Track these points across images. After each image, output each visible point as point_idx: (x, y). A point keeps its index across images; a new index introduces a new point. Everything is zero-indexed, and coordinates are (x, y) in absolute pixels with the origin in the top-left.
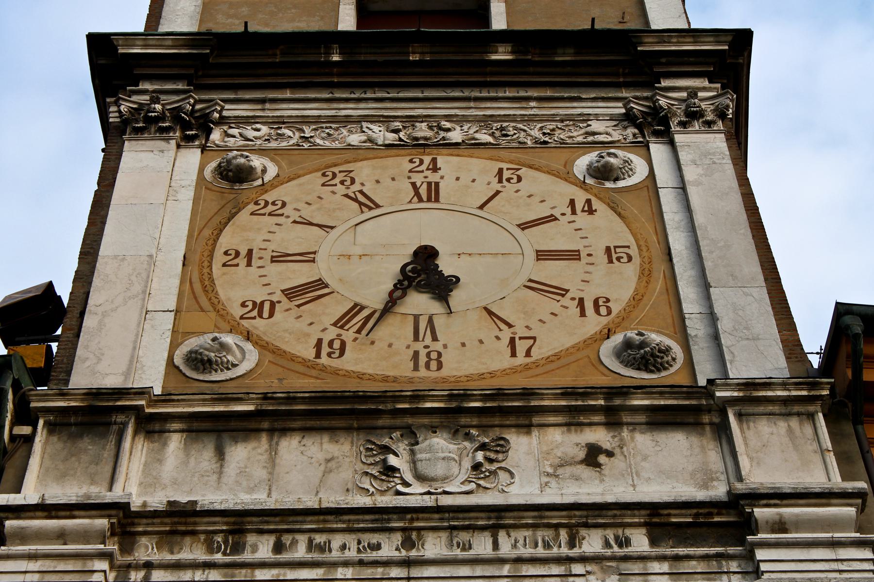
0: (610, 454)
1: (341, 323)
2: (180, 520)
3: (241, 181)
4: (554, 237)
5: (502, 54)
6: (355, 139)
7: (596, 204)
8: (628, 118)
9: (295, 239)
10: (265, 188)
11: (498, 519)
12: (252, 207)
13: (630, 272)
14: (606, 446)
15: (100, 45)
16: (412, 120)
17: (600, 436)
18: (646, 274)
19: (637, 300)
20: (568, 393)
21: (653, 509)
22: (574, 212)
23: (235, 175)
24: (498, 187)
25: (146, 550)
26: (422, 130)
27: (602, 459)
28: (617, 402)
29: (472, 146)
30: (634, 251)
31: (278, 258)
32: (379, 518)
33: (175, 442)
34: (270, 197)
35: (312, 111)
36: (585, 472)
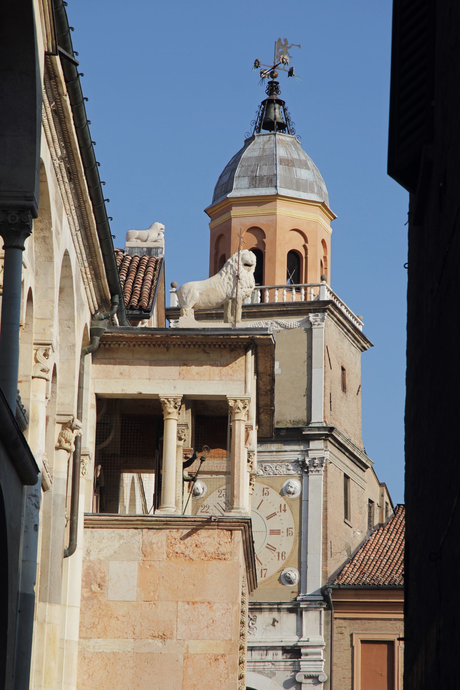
0: (277, 622)
3: (198, 495)
4: (274, 524)
7: (287, 508)
10: (204, 499)
12: (201, 508)
14: (277, 619)
17: (275, 615)
19: (292, 553)
20: (269, 604)
21: (283, 647)
22: (281, 512)
24: (262, 498)
27: (276, 623)
28: (280, 606)
30: (293, 530)
34: (205, 503)
36: (272, 627)
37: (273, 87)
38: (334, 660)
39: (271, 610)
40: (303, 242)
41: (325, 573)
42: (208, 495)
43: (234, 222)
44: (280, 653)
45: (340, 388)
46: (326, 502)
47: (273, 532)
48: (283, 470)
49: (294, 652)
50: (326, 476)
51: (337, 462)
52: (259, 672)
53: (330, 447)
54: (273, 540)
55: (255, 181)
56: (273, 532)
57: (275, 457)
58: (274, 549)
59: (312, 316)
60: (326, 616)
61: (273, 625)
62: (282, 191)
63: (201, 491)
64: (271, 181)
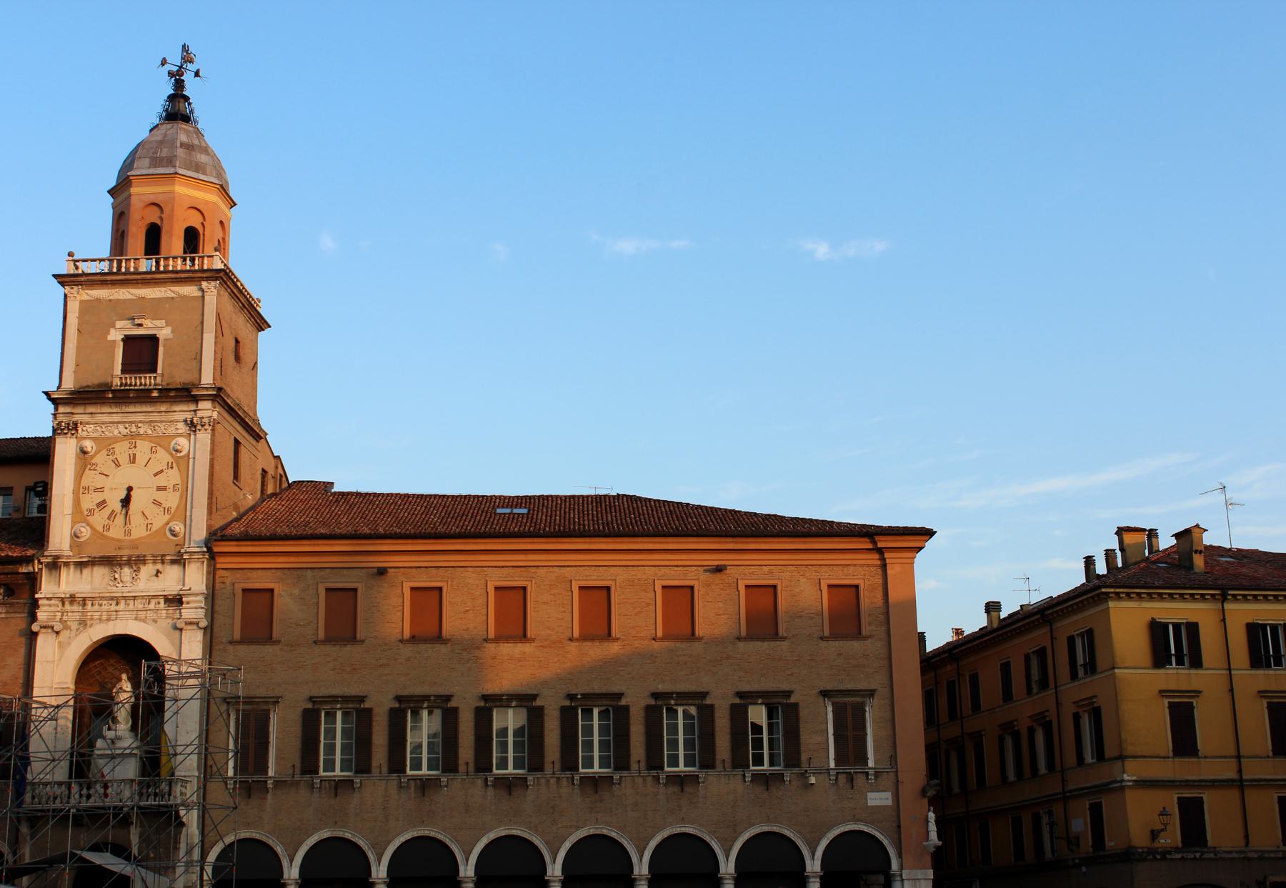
1: (109, 518)
2: (72, 598)
4: (161, 480)
5: (155, 394)
6: (116, 432)
8: (185, 421)
9: (99, 481)
10: (93, 457)
11: (135, 598)
13: (178, 494)
15: (46, 393)
16: (131, 422)
17: (159, 566)
18: (181, 497)
23: (85, 453)
25: (68, 607)
26: (134, 429)
29: (144, 437)
31: (96, 490)
32: (112, 598)
33: (72, 567)
35: (106, 418)
37: (179, 85)
38: (217, 608)
39: (155, 562)
40: (201, 219)
41: (209, 526)
42: (97, 453)
43: (134, 200)
44: (162, 601)
45: (232, 358)
46: (212, 460)
47: (160, 488)
48: (171, 430)
49: (176, 601)
50: (213, 435)
51: (226, 424)
52: (144, 621)
53: (218, 408)
54: (160, 496)
55: (156, 162)
56: (160, 488)
57: (164, 417)
58: (159, 504)
59: (204, 284)
60: (209, 565)
61: (157, 576)
62: (181, 171)
63: (89, 449)
64: (170, 161)
